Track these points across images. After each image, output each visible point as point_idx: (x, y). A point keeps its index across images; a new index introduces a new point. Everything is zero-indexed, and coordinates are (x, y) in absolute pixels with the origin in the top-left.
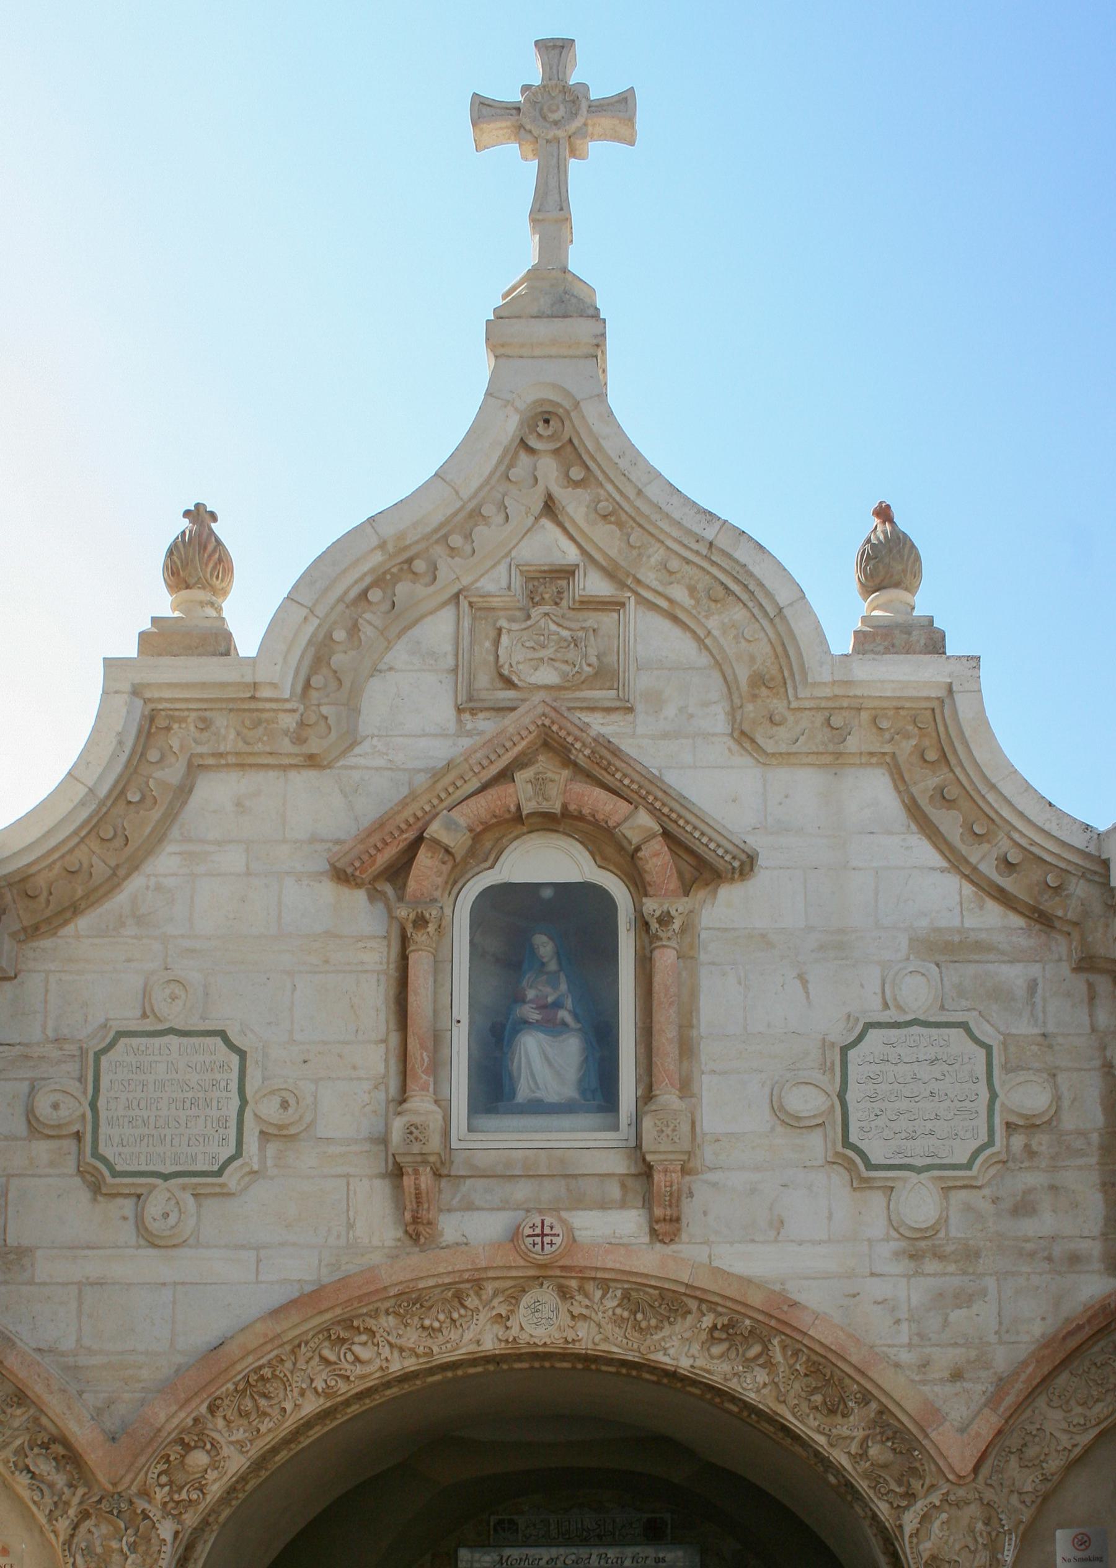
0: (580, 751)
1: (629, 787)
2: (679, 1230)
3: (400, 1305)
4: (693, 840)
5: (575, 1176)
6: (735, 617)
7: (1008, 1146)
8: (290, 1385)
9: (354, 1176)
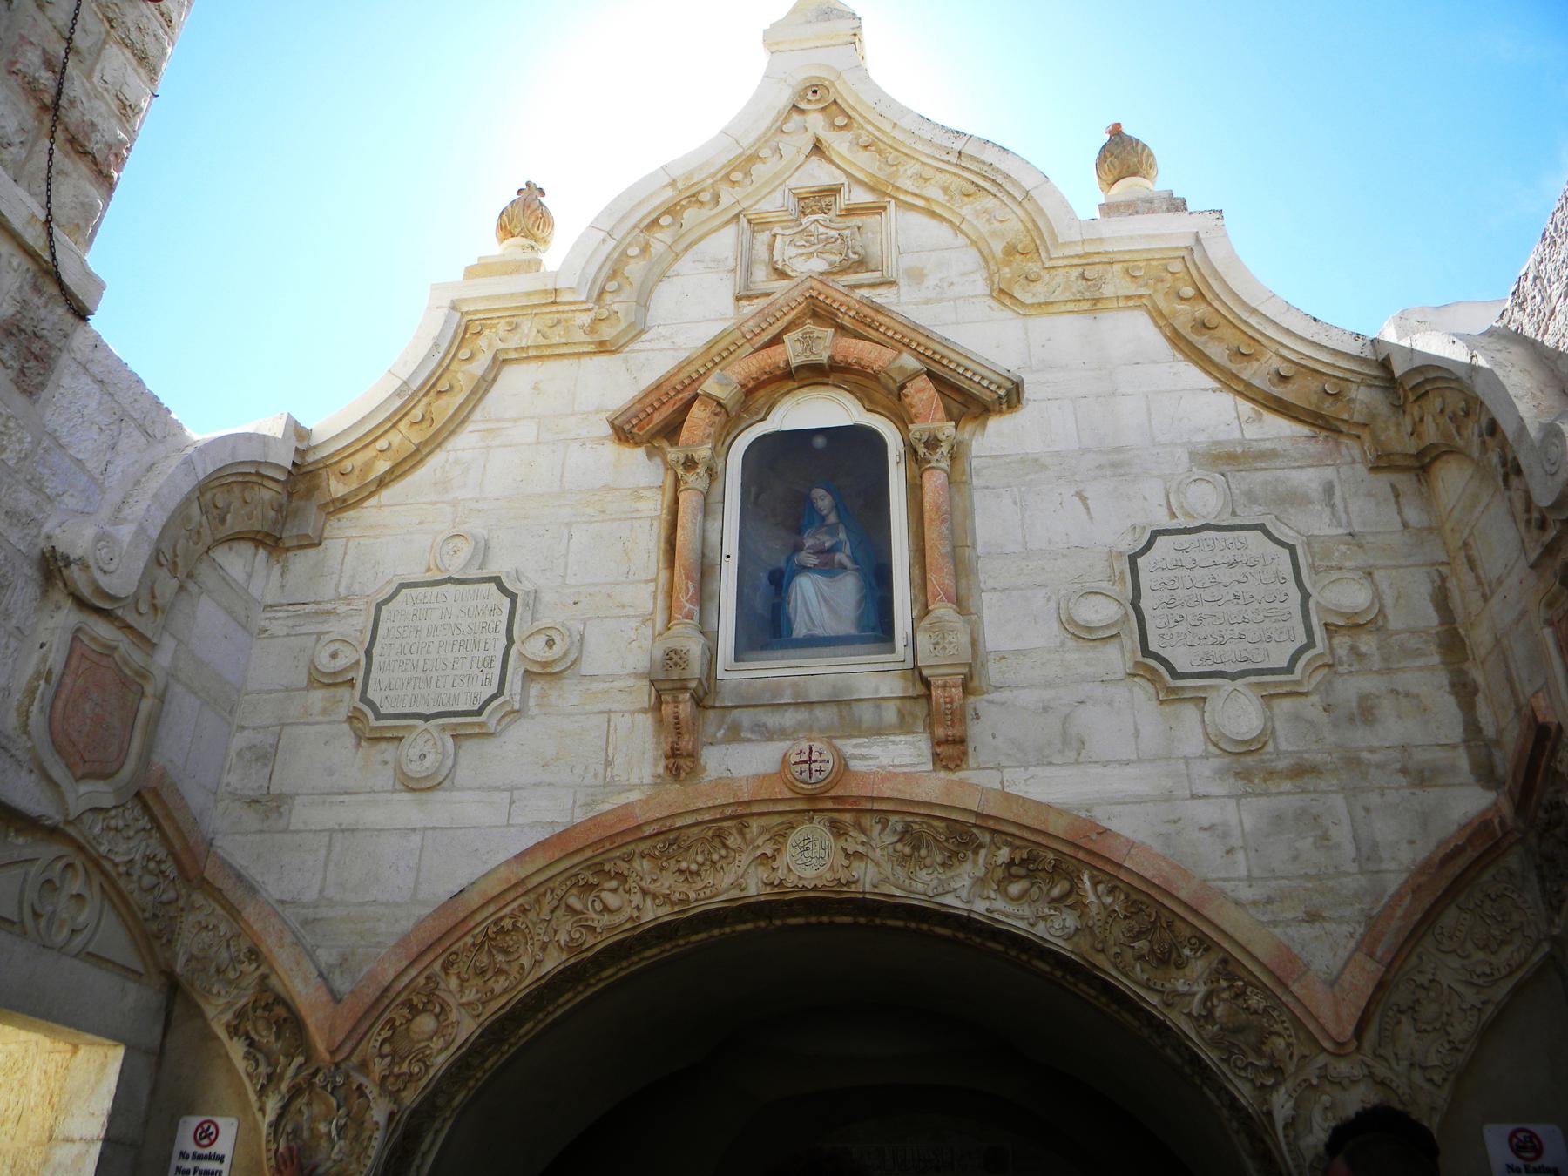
0: (845, 314)
1: (892, 338)
2: (965, 753)
3: (655, 847)
4: (958, 377)
5: (849, 702)
6: (987, 206)
7: (1332, 649)
8: (532, 938)
9: (615, 712)
